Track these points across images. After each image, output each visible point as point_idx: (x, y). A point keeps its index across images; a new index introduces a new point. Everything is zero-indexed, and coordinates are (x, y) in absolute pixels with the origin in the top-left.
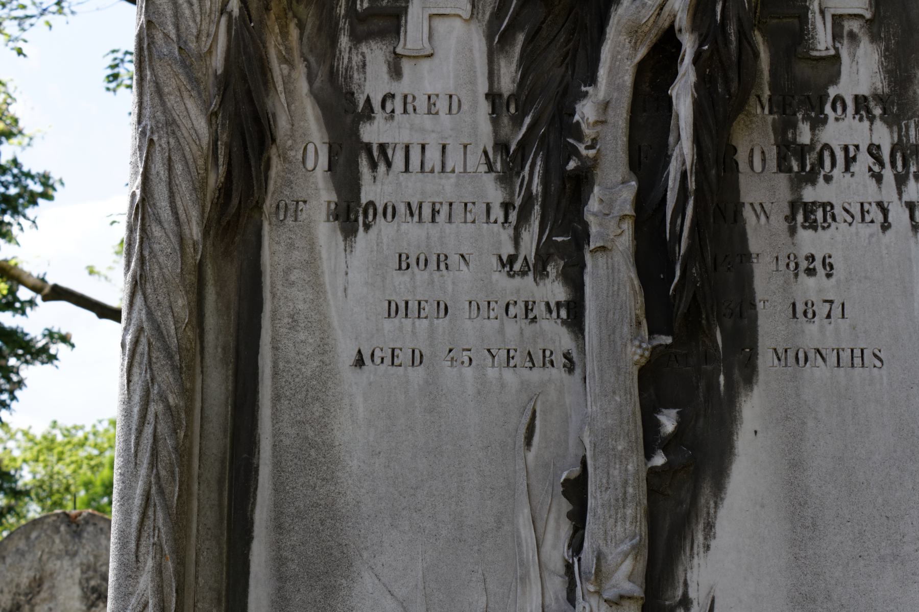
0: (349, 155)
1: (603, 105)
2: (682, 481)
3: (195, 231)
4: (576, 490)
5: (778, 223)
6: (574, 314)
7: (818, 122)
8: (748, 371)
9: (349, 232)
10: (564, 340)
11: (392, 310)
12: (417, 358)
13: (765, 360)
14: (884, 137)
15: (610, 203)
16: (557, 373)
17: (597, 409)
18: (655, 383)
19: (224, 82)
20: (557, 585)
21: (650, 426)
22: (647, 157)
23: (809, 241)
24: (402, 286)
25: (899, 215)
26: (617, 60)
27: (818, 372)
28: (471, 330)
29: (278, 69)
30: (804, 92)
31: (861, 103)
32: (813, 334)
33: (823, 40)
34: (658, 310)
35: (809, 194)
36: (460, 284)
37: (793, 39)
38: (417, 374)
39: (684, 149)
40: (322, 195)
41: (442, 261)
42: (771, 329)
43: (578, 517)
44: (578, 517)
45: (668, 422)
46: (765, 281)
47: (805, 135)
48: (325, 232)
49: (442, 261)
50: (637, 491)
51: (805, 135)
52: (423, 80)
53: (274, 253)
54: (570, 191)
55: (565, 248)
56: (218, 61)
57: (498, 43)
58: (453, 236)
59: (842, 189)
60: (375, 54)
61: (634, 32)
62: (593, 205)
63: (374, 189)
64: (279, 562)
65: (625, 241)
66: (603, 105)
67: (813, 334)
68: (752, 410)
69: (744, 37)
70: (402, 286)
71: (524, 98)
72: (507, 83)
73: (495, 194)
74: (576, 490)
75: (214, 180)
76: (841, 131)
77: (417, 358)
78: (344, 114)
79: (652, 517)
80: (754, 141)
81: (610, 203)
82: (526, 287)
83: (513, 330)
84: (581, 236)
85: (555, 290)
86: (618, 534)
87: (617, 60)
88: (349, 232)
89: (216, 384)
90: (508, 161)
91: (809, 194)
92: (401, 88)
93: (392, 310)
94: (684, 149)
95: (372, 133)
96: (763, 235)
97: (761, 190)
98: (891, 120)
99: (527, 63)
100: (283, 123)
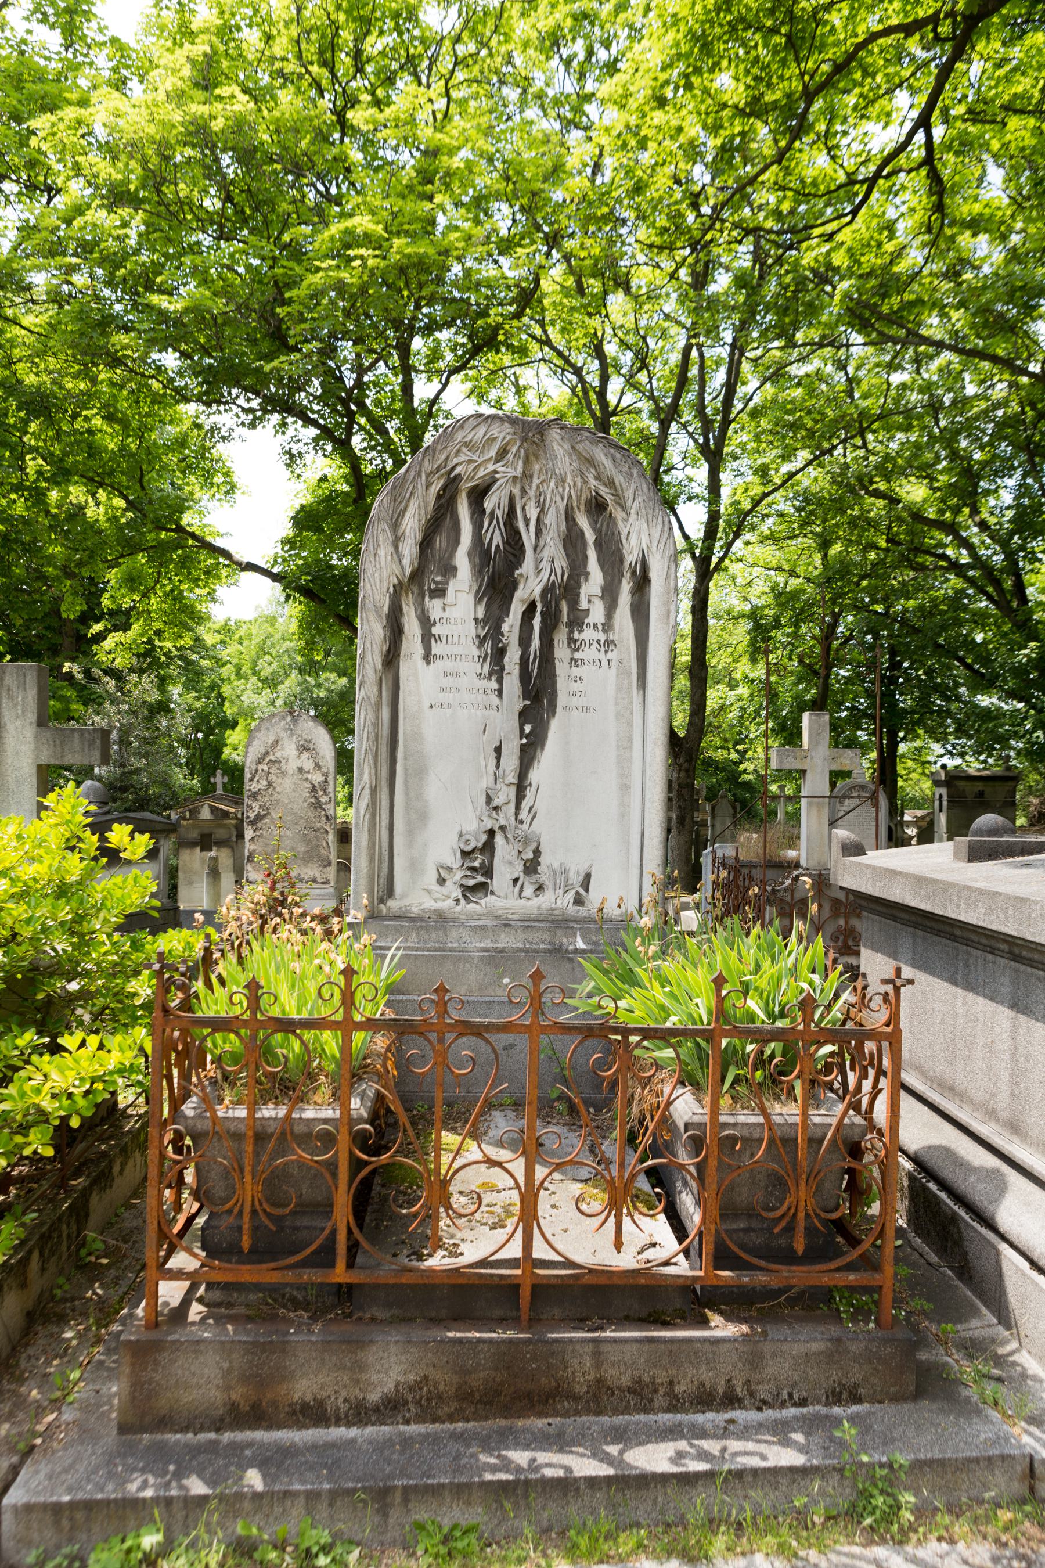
0: (428, 638)
1: (511, 624)
2: (530, 750)
3: (379, 666)
4: (498, 750)
5: (566, 665)
6: (500, 692)
7: (581, 631)
8: (553, 712)
9: (428, 663)
10: (496, 701)
11: (442, 689)
12: (449, 706)
13: (559, 709)
14: (603, 638)
15: (512, 659)
16: (494, 712)
17: (505, 722)
18: (524, 715)
19: (388, 616)
20: (492, 779)
21: (522, 730)
22: (525, 642)
23: (575, 671)
24: (446, 682)
25: (605, 663)
26: (517, 609)
27: (575, 713)
28: (467, 697)
29: (405, 608)
30: (577, 621)
31: (595, 626)
32: (575, 701)
33: (584, 605)
34: (526, 694)
35: (577, 655)
36: (464, 682)
37: (574, 602)
38: (449, 711)
39: (536, 643)
40: (419, 651)
41: (458, 674)
42: (562, 700)
43: (498, 759)
44: (498, 759)
45: (528, 728)
46: (561, 685)
47: (576, 635)
48: (421, 663)
49: (458, 674)
50: (517, 751)
51: (576, 635)
52: (452, 613)
53: (405, 669)
54: (499, 653)
55: (498, 672)
56: (386, 609)
57: (478, 600)
58: (463, 666)
59: (586, 654)
60: (437, 603)
61: (523, 601)
62: (506, 659)
63: (436, 649)
64: (406, 770)
65: (516, 671)
66: (511, 624)
67: (575, 701)
68: (554, 725)
69: (557, 605)
70: (446, 682)
71: (485, 621)
72: (481, 615)
73: (476, 652)
74: (498, 750)
75: (385, 648)
76: (588, 634)
77: (449, 706)
78: (426, 622)
79: (521, 759)
80: (560, 637)
81: (512, 659)
82: (484, 683)
83: (480, 697)
84: (503, 669)
85: (495, 685)
86: (511, 762)
87: (517, 609)
88: (428, 663)
89: (386, 713)
90: (481, 641)
91: (577, 655)
92: (445, 615)
93: (442, 689)
94: (536, 643)
95: (435, 630)
96: (562, 668)
97: (561, 652)
98: (605, 631)
99: (488, 608)
100: (406, 628)
